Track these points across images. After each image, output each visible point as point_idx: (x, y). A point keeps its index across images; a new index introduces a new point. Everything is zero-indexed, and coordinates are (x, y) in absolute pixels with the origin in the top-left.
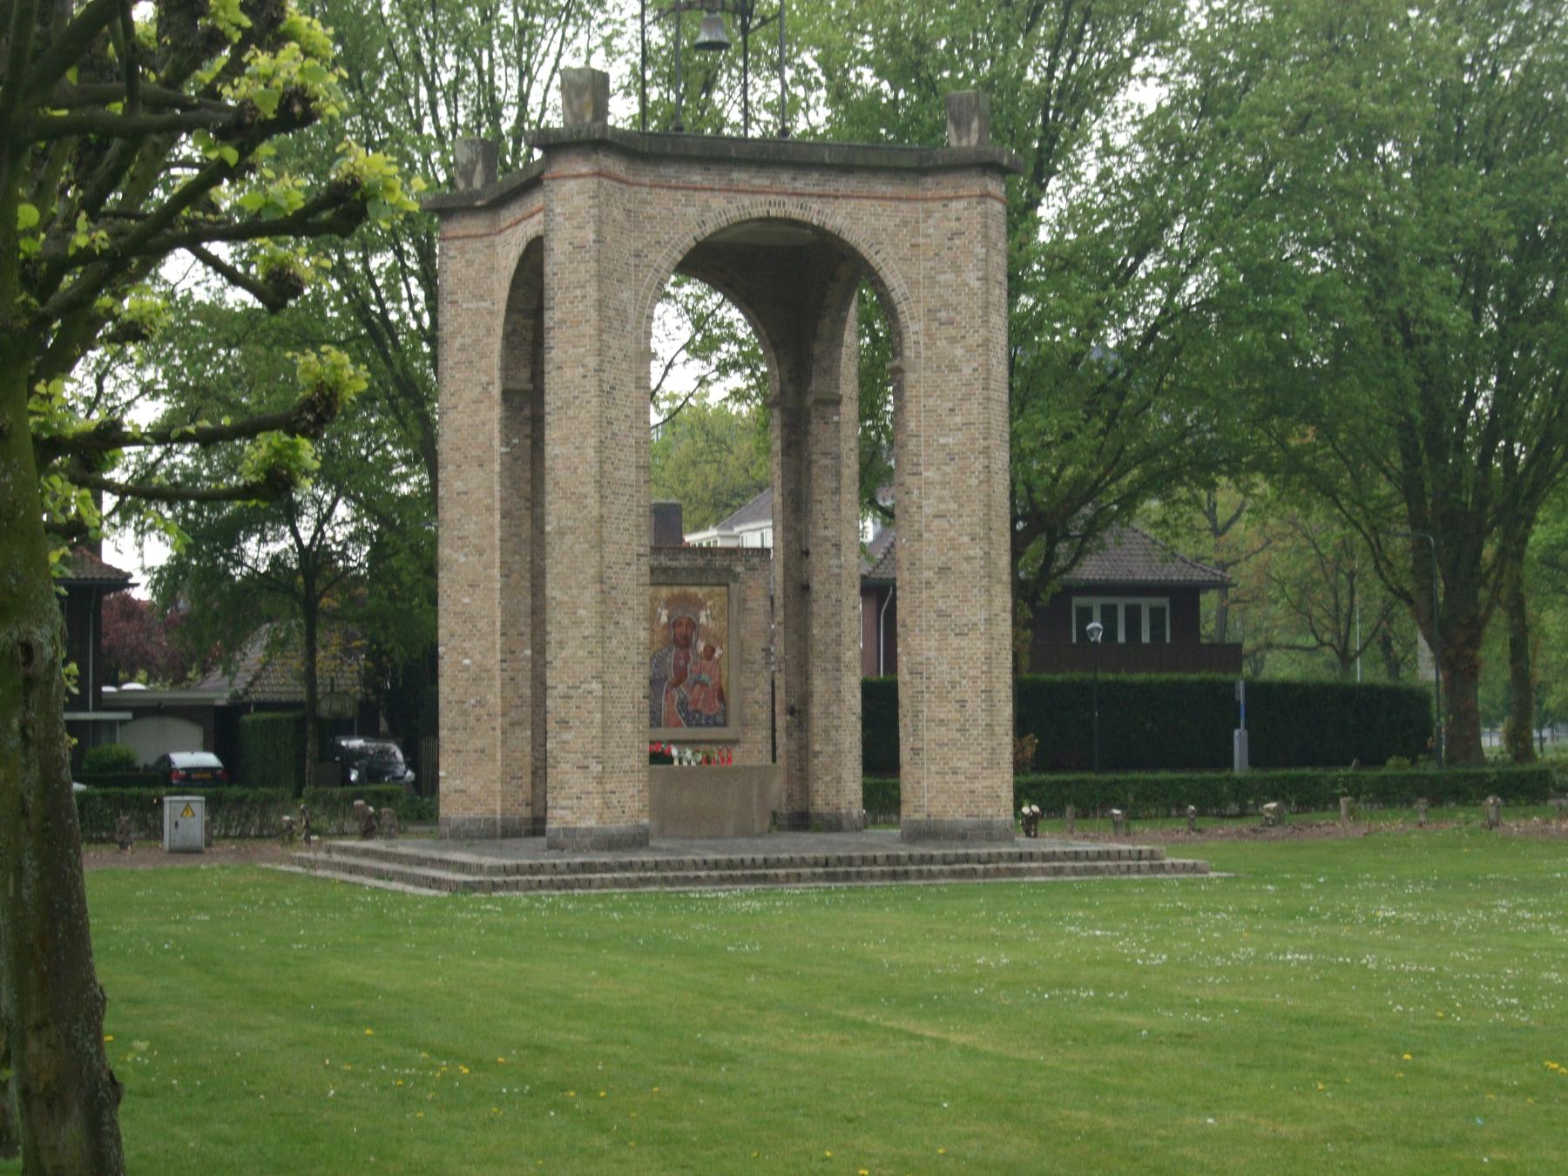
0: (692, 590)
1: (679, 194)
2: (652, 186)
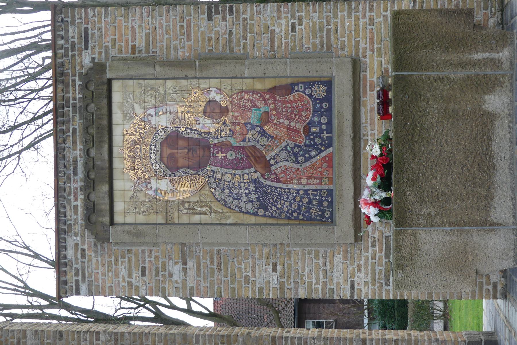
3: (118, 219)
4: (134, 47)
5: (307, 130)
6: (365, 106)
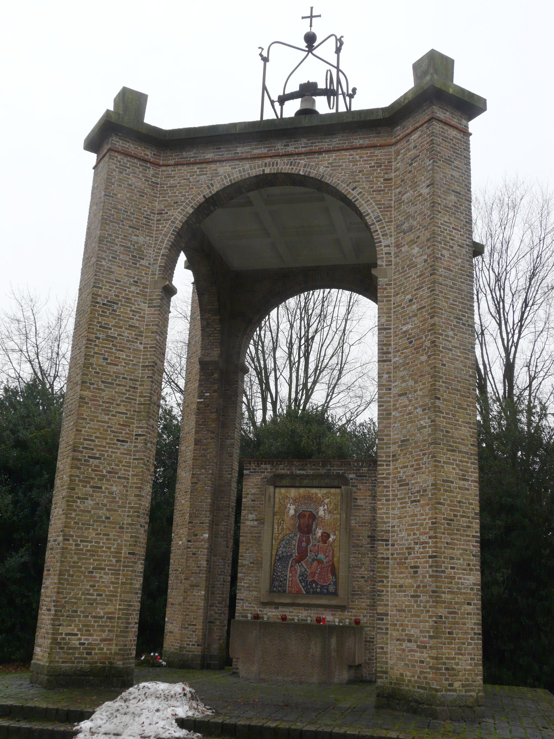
0: (314, 491)
1: (195, 168)
2: (176, 164)
3: (277, 490)
4: (356, 499)
5: (314, 581)
6: (325, 610)
